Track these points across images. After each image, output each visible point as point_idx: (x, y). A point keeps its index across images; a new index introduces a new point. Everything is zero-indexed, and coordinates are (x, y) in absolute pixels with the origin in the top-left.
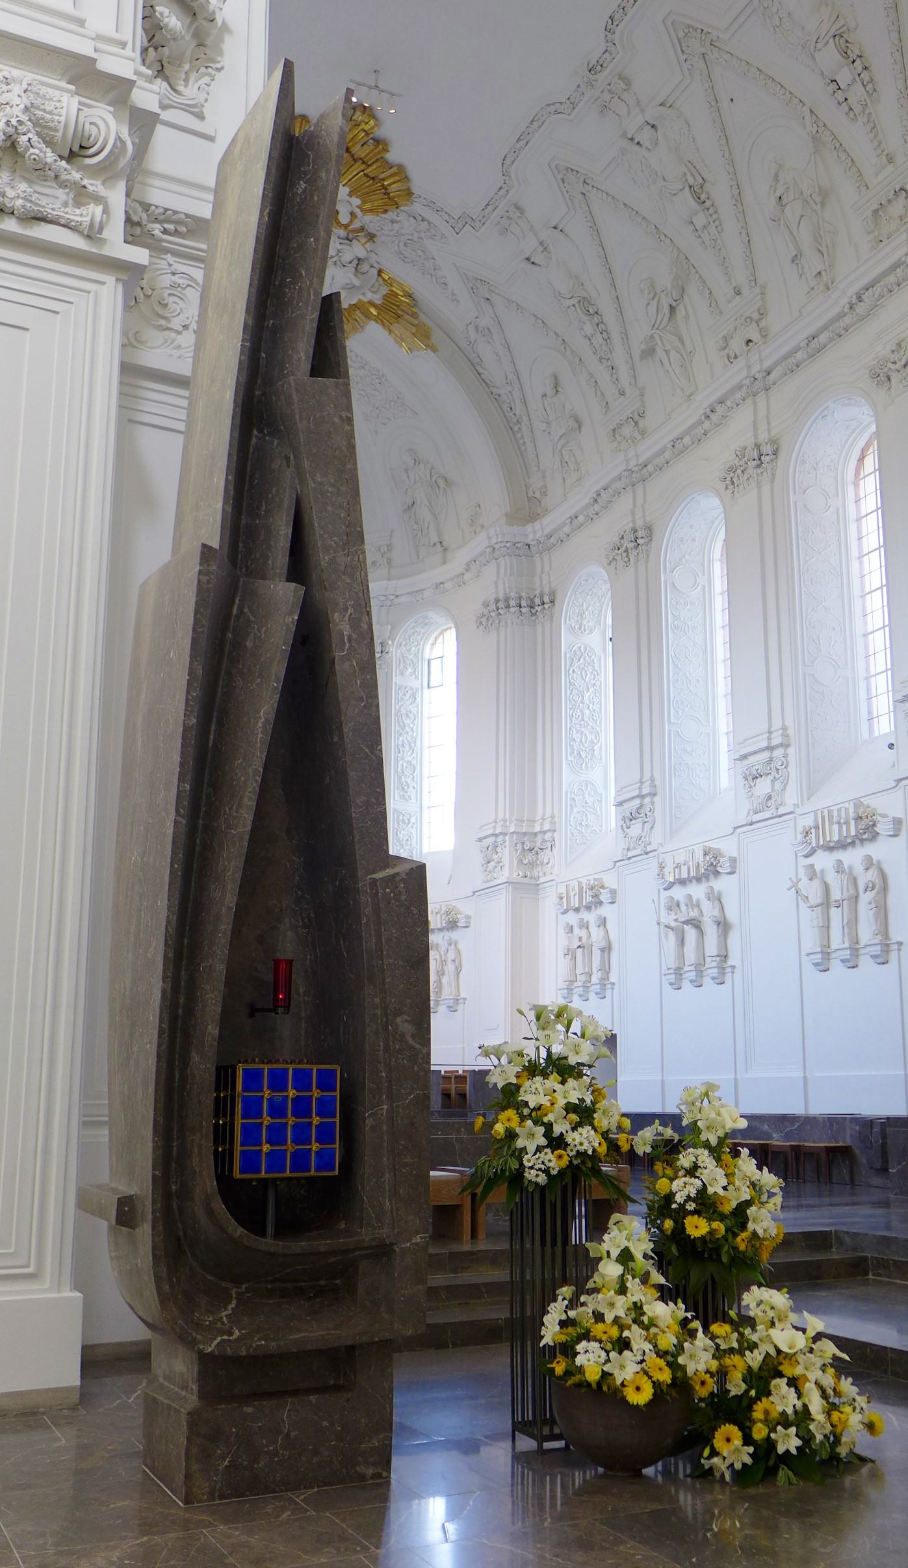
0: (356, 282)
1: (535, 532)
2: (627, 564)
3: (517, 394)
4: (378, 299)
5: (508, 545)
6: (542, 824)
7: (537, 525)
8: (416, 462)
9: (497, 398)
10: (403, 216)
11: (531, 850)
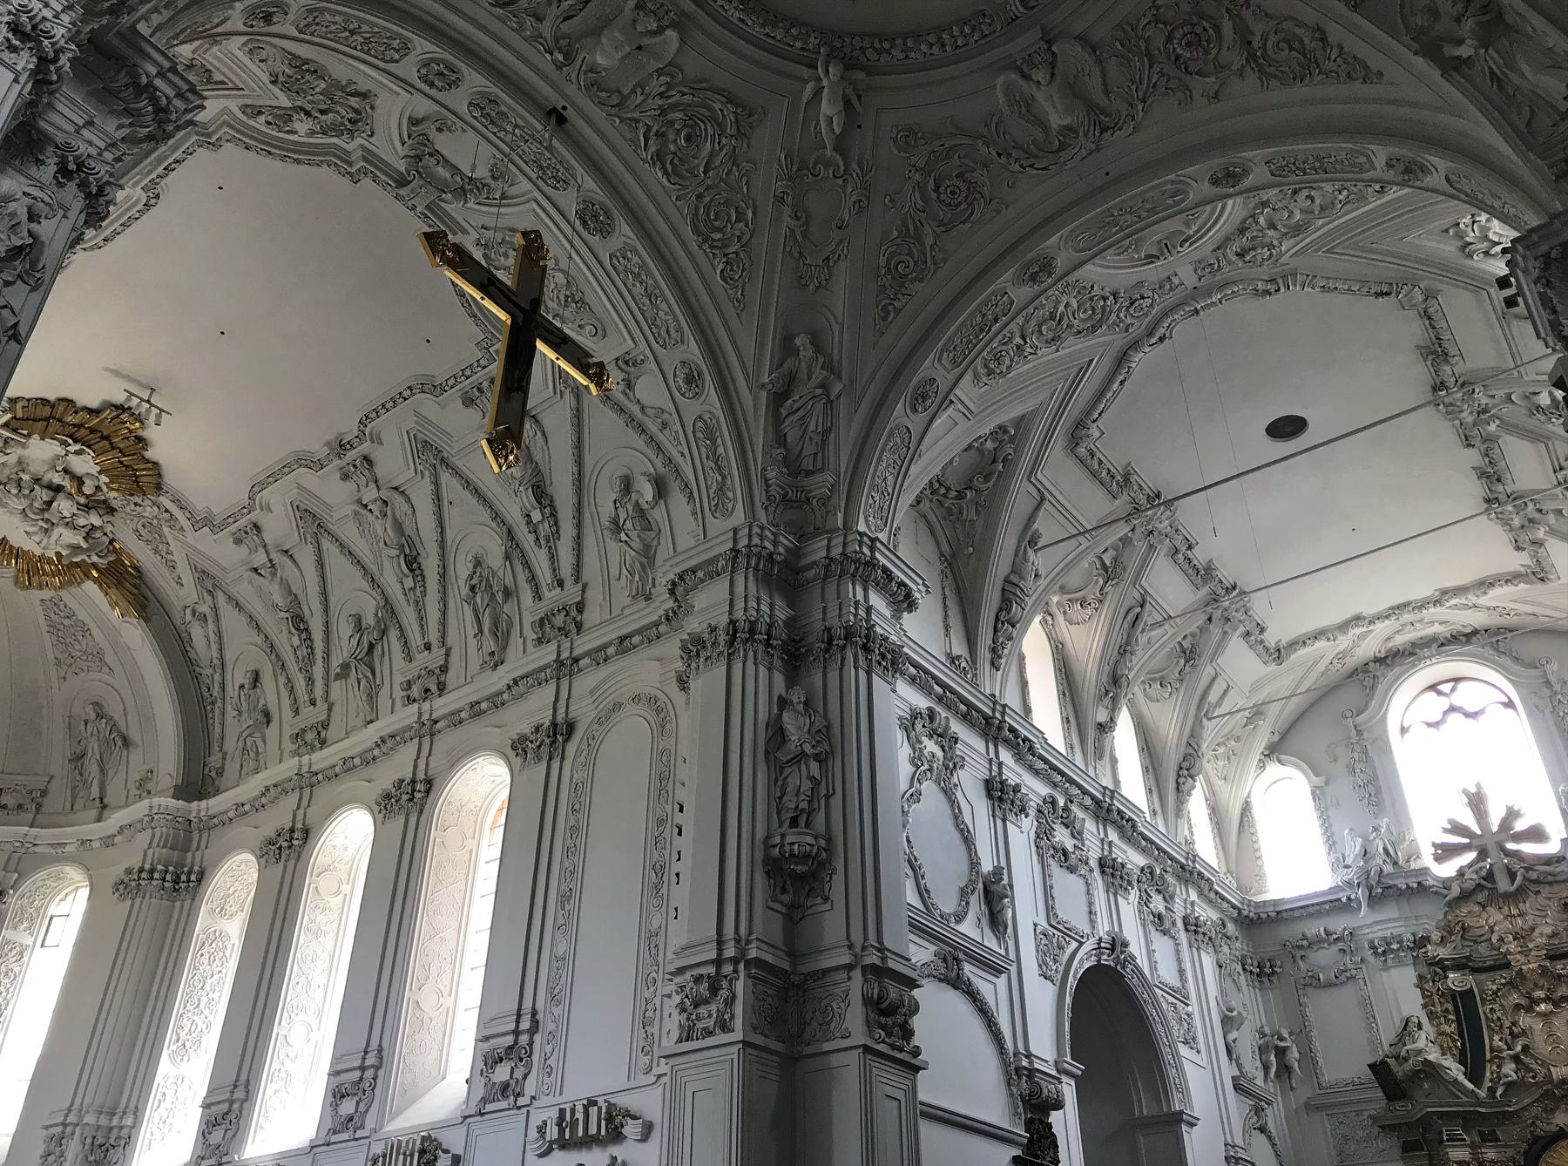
0: (84, 545)
1: (199, 811)
2: (278, 860)
3: (217, 677)
4: (102, 562)
5: (168, 817)
6: (121, 1118)
7: (203, 804)
8: (99, 716)
9: (197, 677)
10: (147, 502)
11: (100, 1146)
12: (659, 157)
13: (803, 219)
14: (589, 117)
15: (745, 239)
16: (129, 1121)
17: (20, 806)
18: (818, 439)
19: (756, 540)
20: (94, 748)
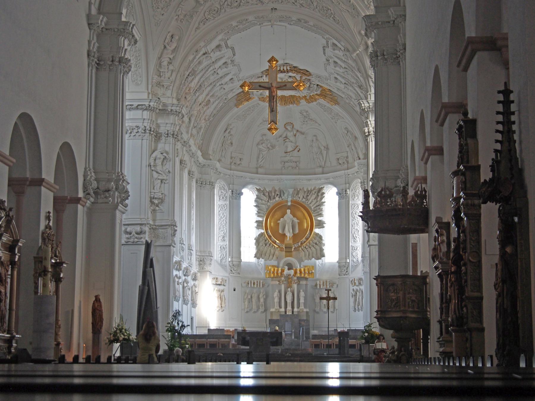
4: (319, 92)
5: (362, 165)
13: (341, 3)
15: (333, 14)
17: (344, 163)
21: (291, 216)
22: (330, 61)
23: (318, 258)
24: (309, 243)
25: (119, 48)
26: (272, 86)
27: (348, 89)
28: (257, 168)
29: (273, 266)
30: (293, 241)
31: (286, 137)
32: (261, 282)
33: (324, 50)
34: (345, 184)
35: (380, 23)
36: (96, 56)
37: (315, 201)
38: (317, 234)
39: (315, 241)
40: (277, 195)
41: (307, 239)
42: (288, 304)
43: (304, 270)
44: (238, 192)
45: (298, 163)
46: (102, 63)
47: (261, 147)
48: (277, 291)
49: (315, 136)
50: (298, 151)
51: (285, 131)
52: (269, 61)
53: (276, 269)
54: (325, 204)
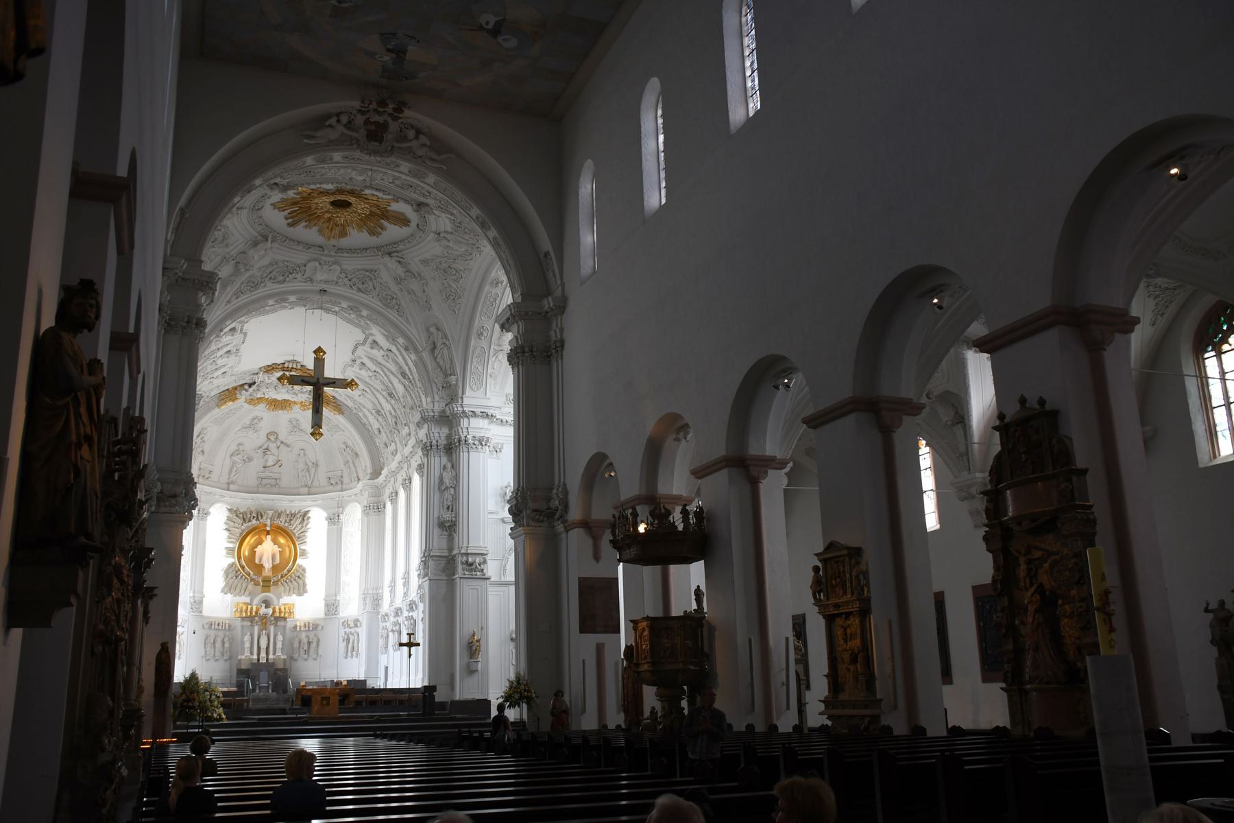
12: (359, 290)
13: (412, 292)
14: (331, 288)
16: (381, 591)
17: (337, 483)
18: (449, 362)
19: (426, 414)
20: (349, 459)
21: (272, 544)
22: (357, 362)
23: (300, 594)
24: (291, 576)
25: (198, 307)
26: (318, 382)
27: (365, 397)
28: (228, 484)
29: (245, 603)
30: (273, 574)
31: (267, 449)
32: (227, 622)
33: (356, 348)
34: (338, 507)
35: (530, 313)
36: (169, 312)
37: (300, 526)
38: (300, 566)
39: (298, 574)
40: (254, 517)
41: (289, 571)
42: (262, 650)
43: (285, 609)
44: (205, 512)
45: (278, 480)
46: (172, 323)
47: (235, 458)
48: (249, 633)
49: (302, 450)
50: (280, 466)
51: (267, 441)
52: (315, 352)
53: (249, 607)
54: (309, 530)
